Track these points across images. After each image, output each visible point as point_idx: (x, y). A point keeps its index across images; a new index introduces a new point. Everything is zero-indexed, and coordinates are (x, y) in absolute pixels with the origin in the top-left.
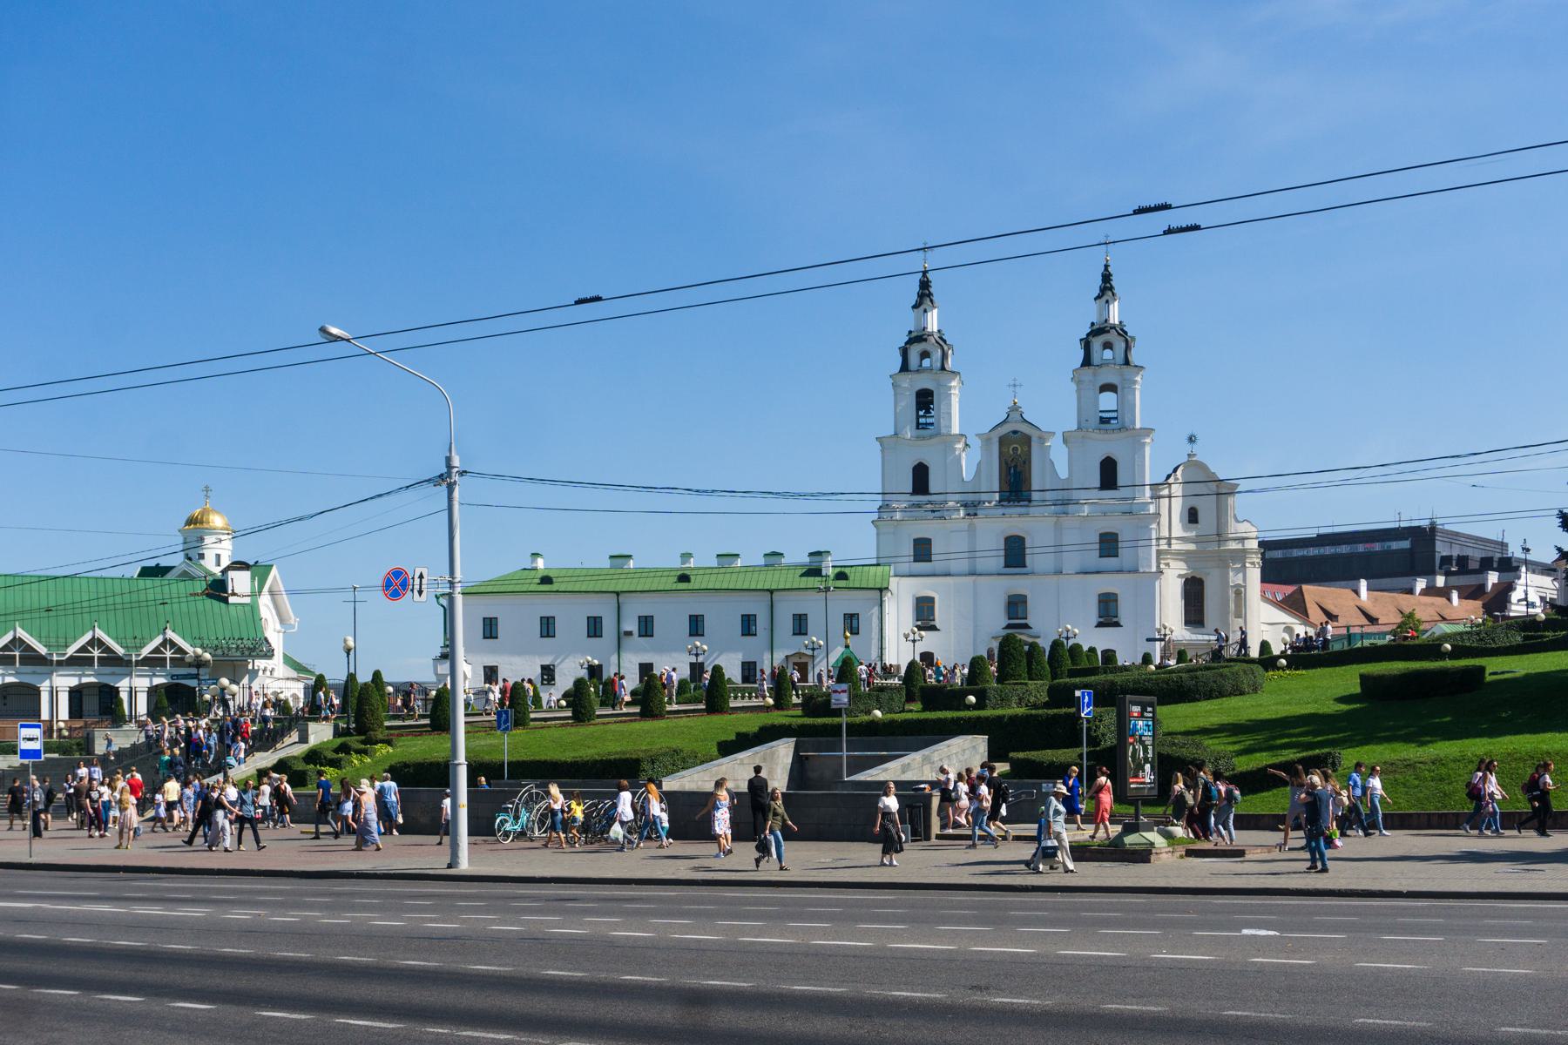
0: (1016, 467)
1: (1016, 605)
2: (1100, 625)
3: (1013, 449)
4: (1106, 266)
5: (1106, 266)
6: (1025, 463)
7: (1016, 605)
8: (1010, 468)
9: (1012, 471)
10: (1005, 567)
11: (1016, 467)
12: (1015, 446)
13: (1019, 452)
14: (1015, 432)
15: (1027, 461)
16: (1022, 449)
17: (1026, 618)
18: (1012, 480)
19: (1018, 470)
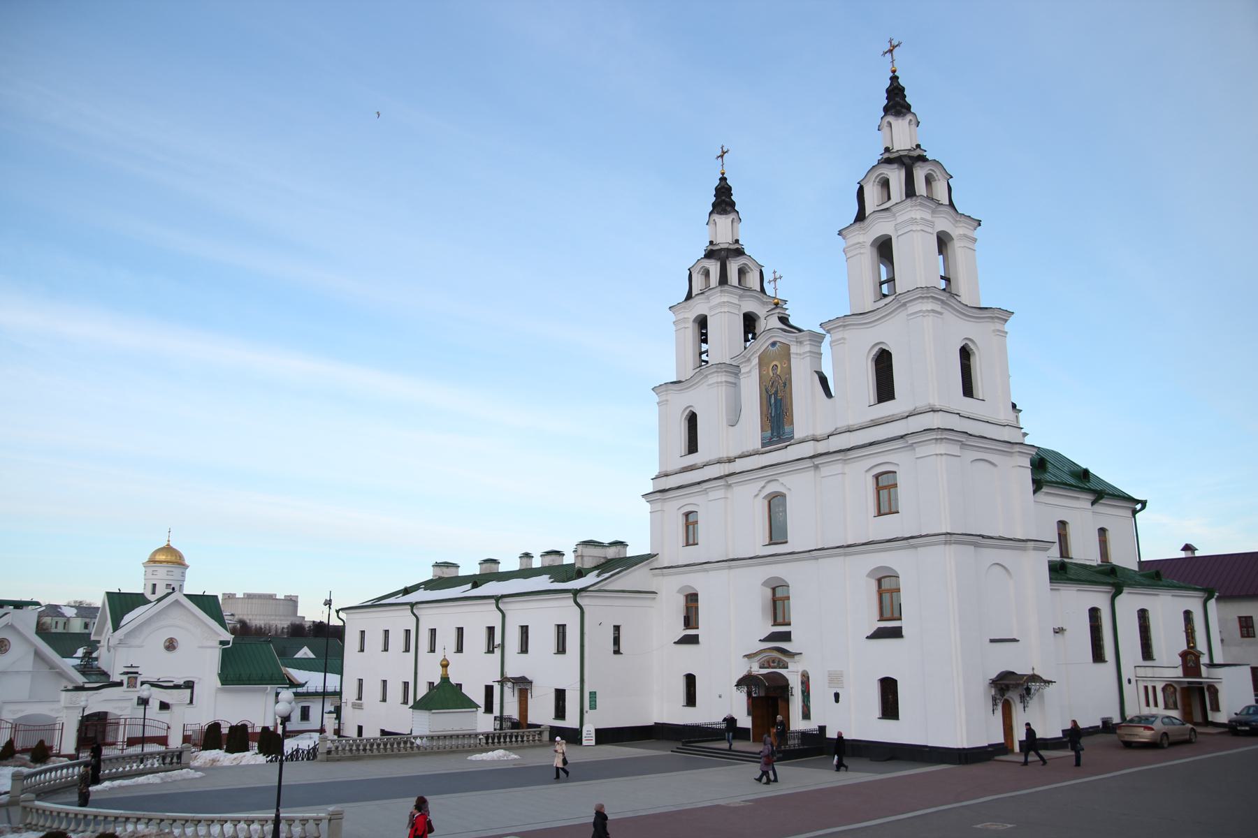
0: (776, 393)
1: (778, 604)
2: (880, 634)
3: (776, 366)
4: (894, 79)
5: (894, 79)
6: (785, 384)
7: (778, 604)
8: (770, 396)
9: (773, 401)
10: (769, 544)
11: (776, 393)
12: (774, 363)
13: (778, 373)
14: (774, 344)
15: (787, 384)
16: (782, 367)
17: (789, 624)
18: (773, 415)
19: (780, 394)
